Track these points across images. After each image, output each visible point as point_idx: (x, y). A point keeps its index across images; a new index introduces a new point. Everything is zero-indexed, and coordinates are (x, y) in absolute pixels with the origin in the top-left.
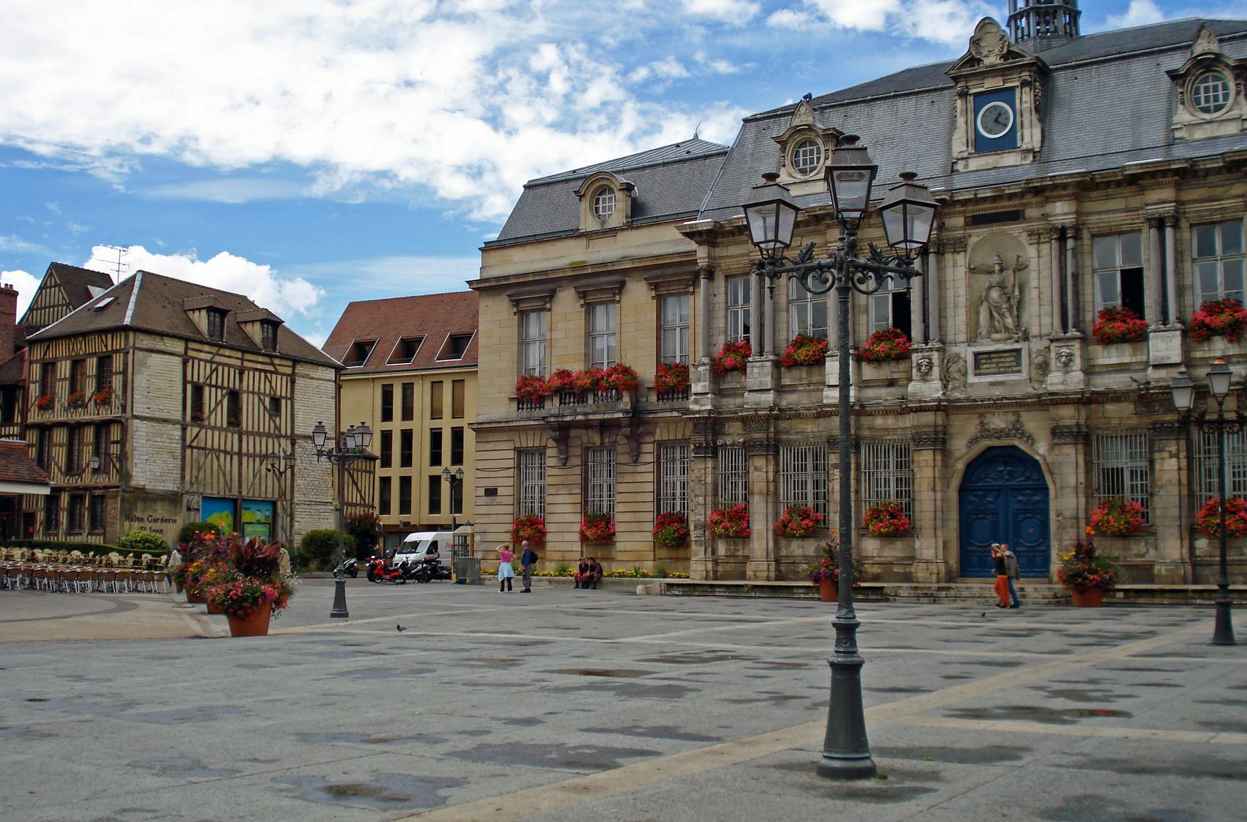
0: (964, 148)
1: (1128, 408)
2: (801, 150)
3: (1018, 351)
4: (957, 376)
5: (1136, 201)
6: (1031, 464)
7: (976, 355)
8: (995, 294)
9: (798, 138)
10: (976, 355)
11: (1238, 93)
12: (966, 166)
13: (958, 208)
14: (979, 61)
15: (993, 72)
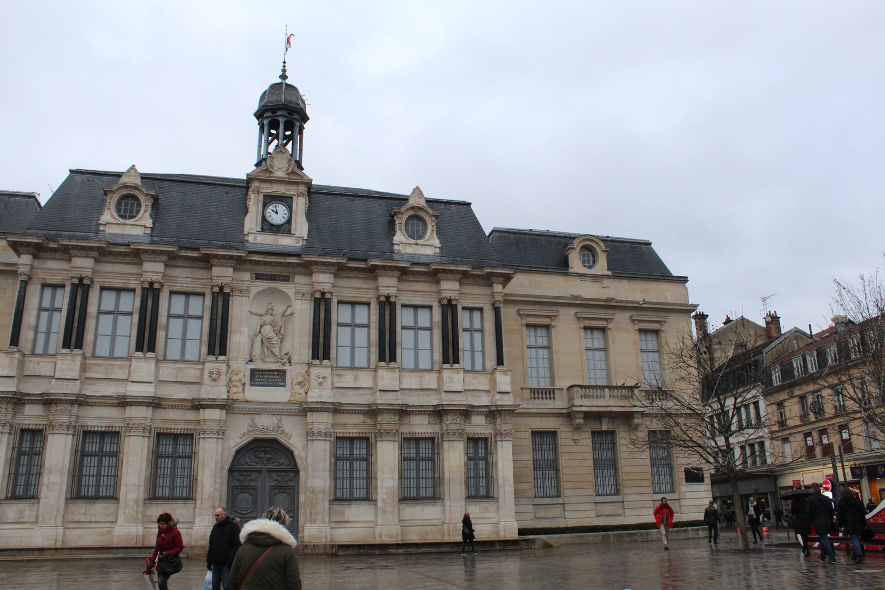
0: (254, 226)
1: (359, 419)
2: (124, 202)
3: (284, 372)
4: (238, 384)
5: (371, 284)
6: (289, 453)
7: (252, 371)
8: (267, 329)
9: (125, 192)
10: (252, 371)
11: (432, 231)
12: (255, 239)
13: (248, 266)
14: (271, 172)
15: (279, 181)
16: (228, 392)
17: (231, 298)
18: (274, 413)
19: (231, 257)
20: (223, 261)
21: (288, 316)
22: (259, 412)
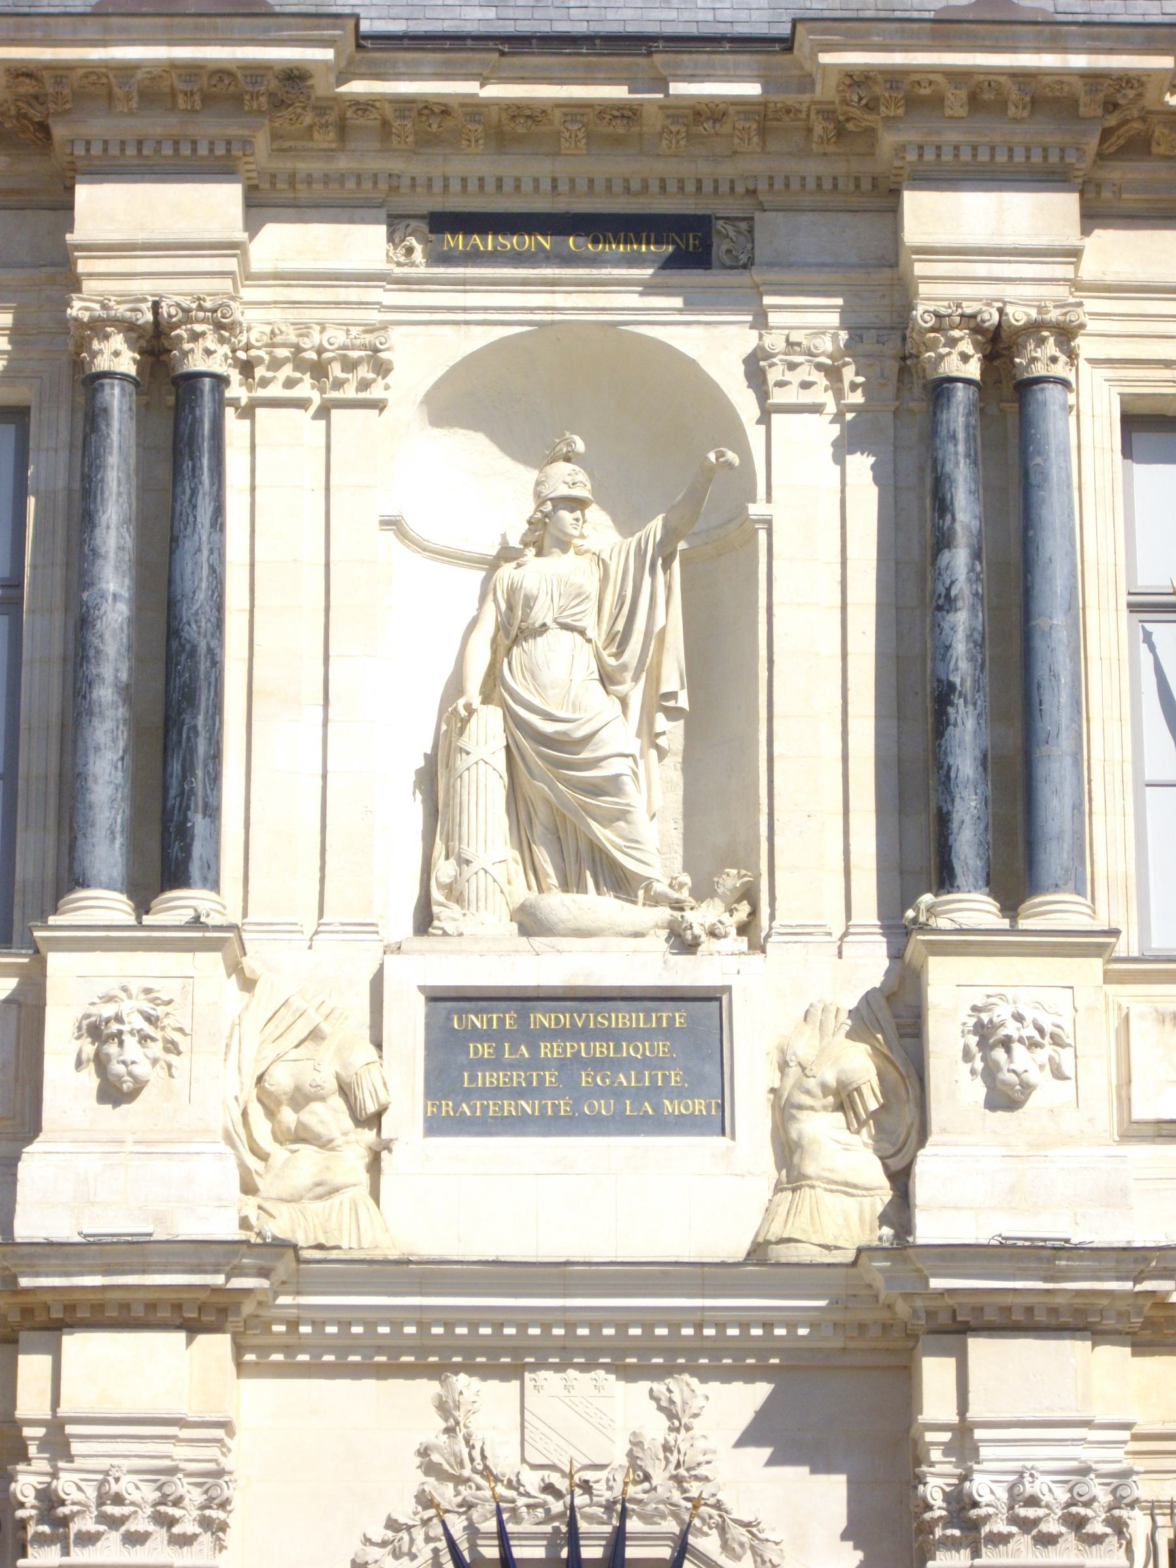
4: (329, 1116)
16: (249, 1188)
17: (235, 428)
18: (632, 1357)
19: (221, 89)
20: (156, 125)
21: (710, 543)
22: (508, 1360)
